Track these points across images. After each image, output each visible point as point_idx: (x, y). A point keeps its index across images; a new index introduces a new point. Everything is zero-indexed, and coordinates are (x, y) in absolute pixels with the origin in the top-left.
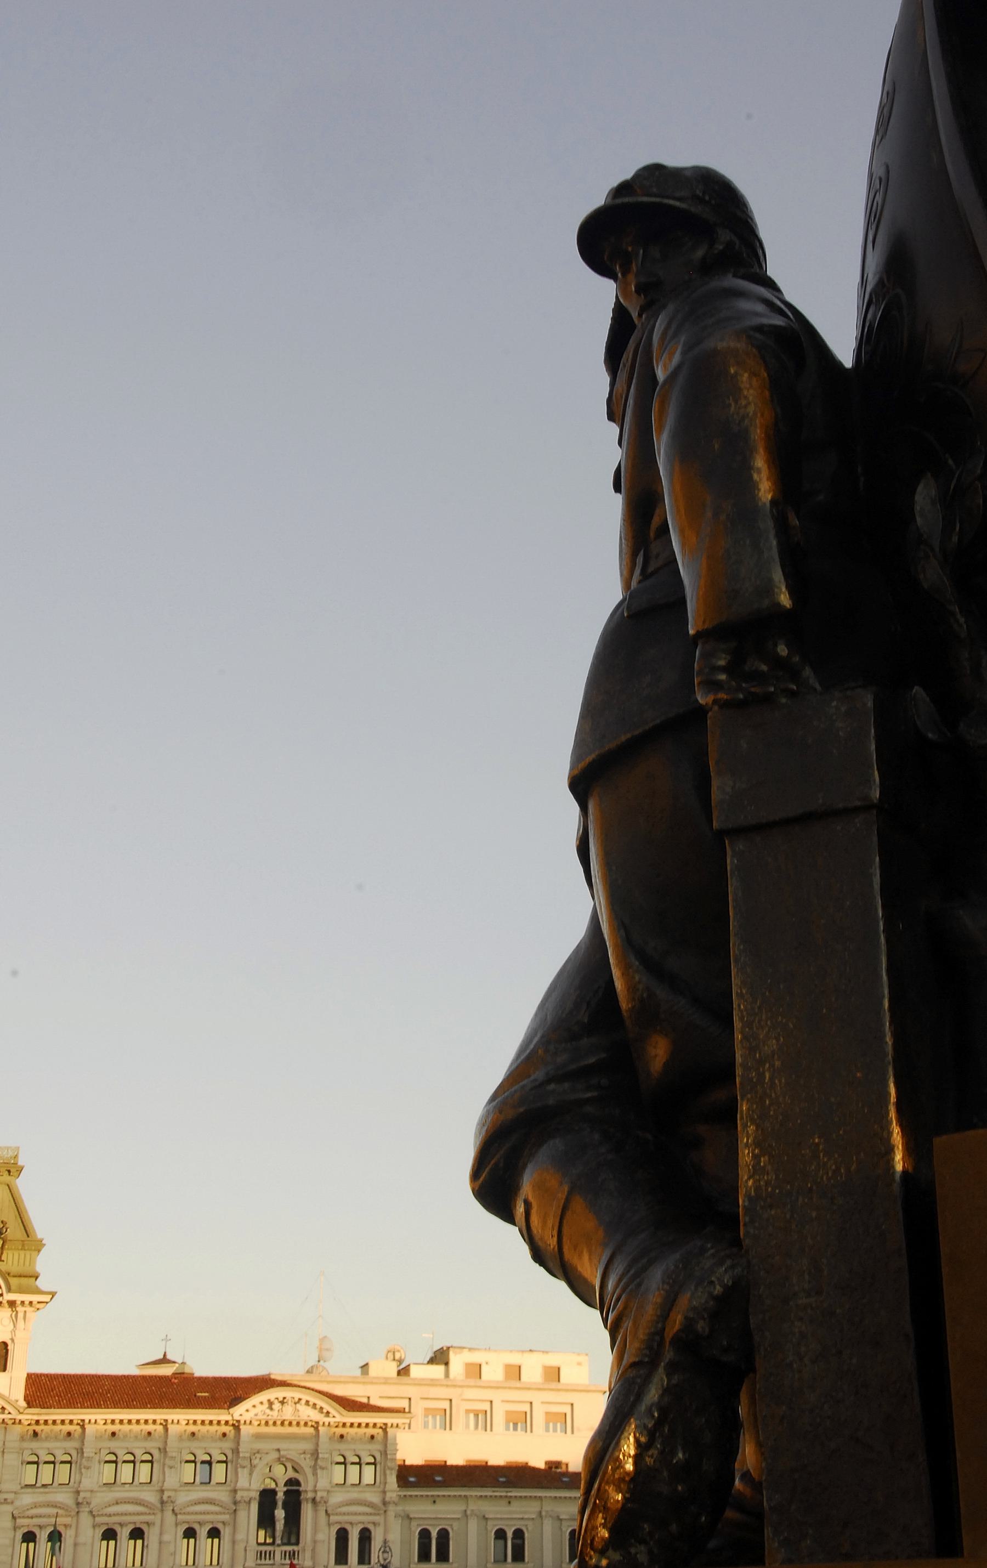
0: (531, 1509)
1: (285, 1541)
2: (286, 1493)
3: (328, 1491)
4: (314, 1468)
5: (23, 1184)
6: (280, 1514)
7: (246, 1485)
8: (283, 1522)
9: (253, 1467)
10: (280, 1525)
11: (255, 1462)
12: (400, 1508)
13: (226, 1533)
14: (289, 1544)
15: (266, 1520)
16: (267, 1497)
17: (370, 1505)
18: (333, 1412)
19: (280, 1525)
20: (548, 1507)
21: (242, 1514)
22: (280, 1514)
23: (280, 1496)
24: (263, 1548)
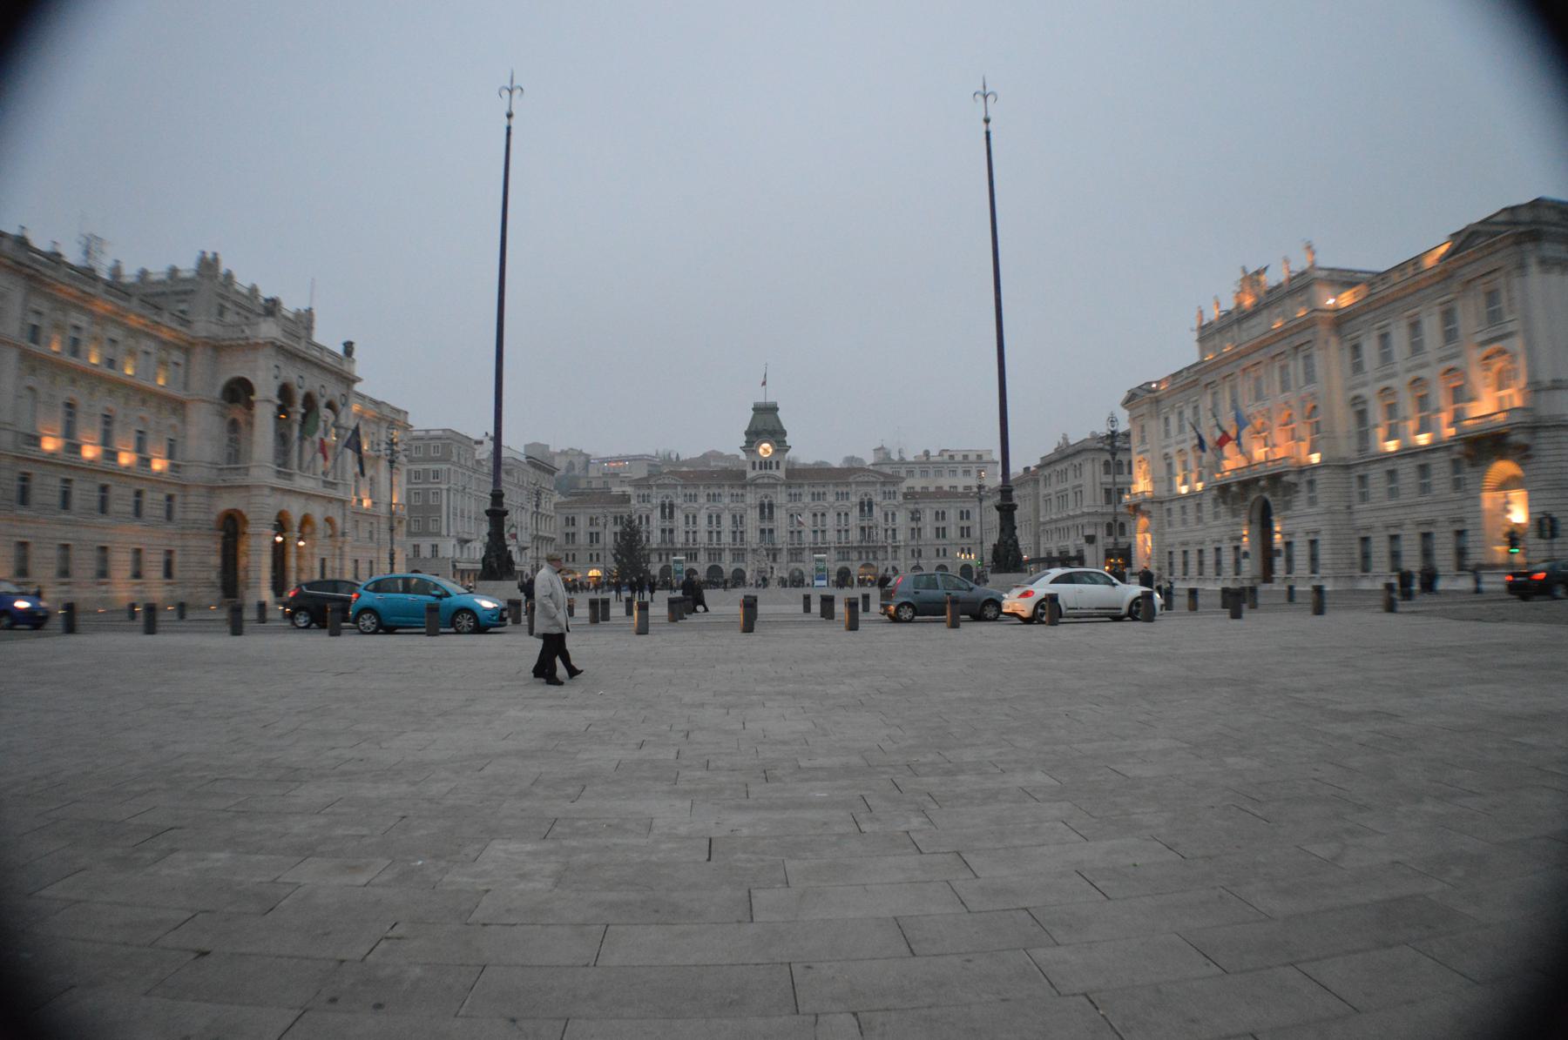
5: (779, 413)
15: (862, 510)
16: (862, 504)
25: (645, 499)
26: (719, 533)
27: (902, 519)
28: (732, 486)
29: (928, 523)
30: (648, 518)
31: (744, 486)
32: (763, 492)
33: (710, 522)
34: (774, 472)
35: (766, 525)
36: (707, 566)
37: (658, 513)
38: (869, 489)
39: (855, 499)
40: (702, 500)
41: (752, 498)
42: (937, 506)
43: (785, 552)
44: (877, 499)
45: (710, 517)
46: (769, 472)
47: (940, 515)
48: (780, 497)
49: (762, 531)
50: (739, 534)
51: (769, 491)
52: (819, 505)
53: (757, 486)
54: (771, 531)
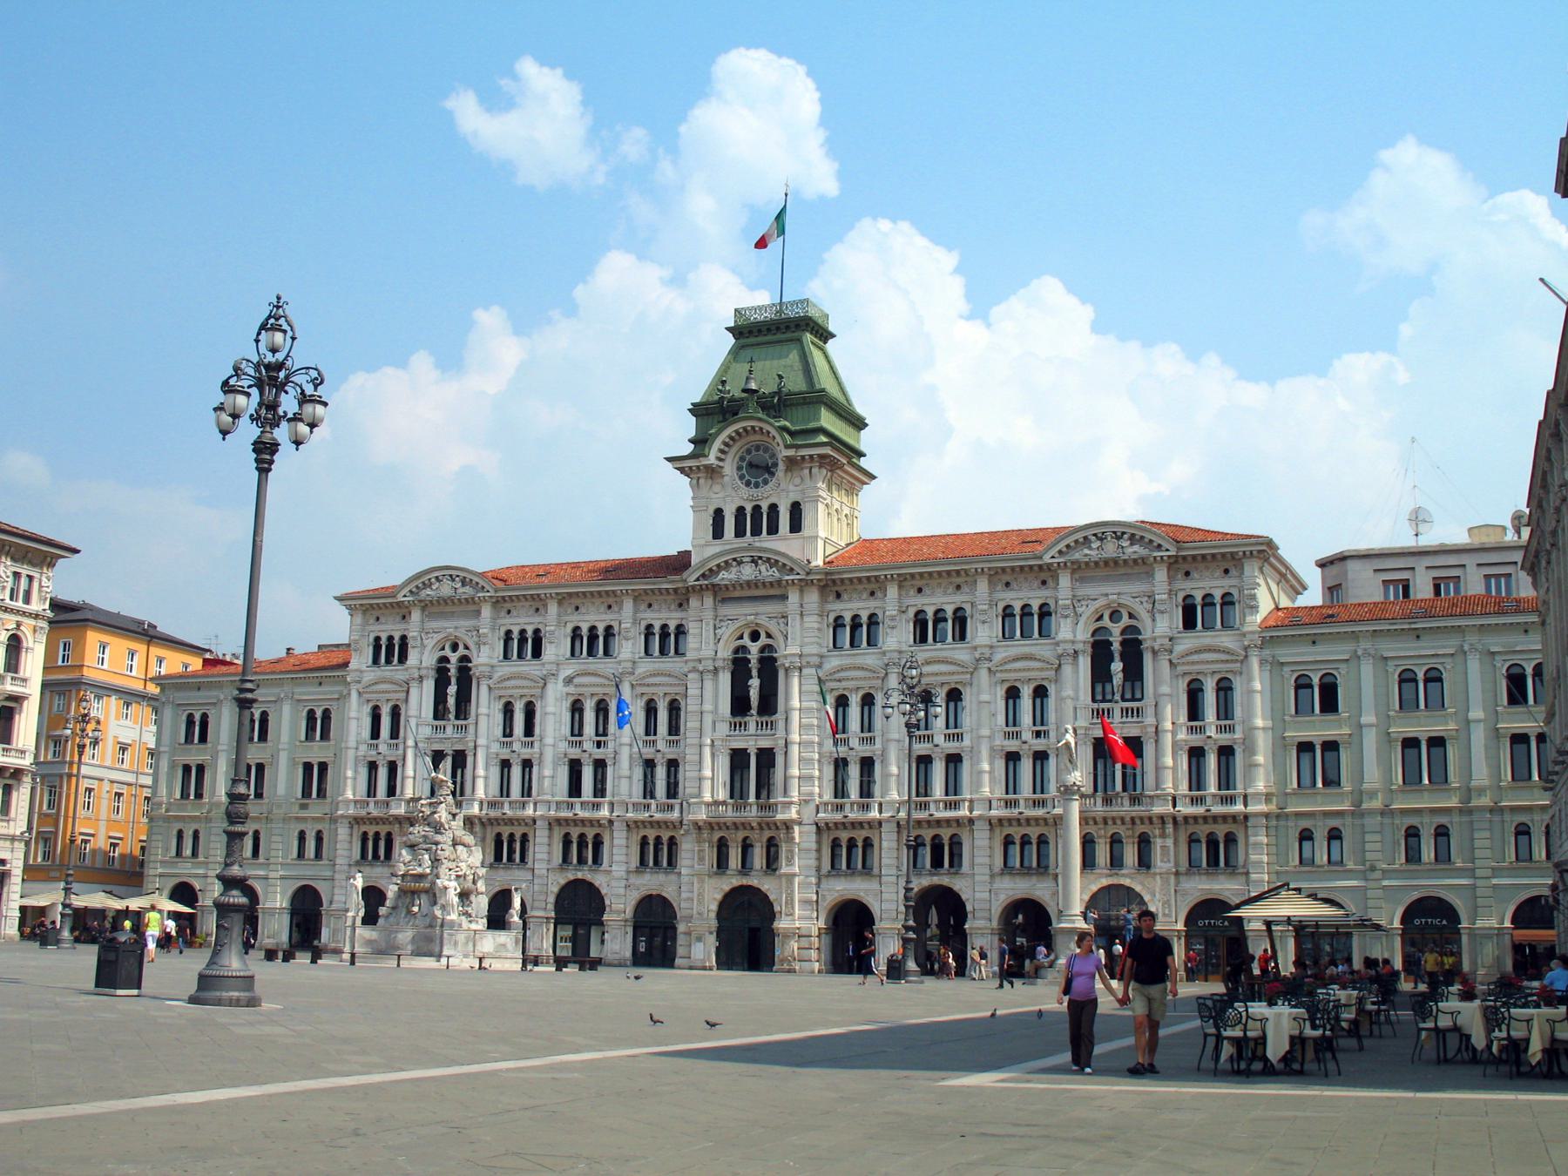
0: (1448, 646)
1: (1128, 696)
2: (1123, 643)
3: (822, 657)
4: (1152, 612)
6: (1117, 666)
7: (1069, 636)
8: (1121, 675)
9: (1077, 616)
10: (1118, 679)
11: (1079, 610)
12: (1267, 652)
13: (1052, 690)
14: (1133, 699)
16: (1100, 652)
17: (1226, 651)
18: (1165, 545)
19: (1118, 679)
20: (1365, 644)
21: (1067, 670)
22: (1117, 666)
23: (1116, 647)
24: (1103, 705)
25: (392, 651)
26: (600, 765)
27: (1260, 704)
28: (644, 599)
29: (1369, 721)
30: (395, 713)
31: (682, 600)
32: (746, 614)
33: (577, 729)
34: (784, 544)
35: (752, 739)
36: (557, 881)
37: (421, 701)
38: (1125, 592)
39: (1073, 632)
40: (556, 648)
41: (711, 637)
42: (1418, 653)
43: (803, 837)
44: (1161, 627)
45: (577, 708)
46: (766, 542)
47: (1420, 687)
48: (801, 635)
49: (738, 759)
50: (663, 777)
51: (762, 615)
52: (941, 662)
53: (725, 596)
54: (767, 758)
